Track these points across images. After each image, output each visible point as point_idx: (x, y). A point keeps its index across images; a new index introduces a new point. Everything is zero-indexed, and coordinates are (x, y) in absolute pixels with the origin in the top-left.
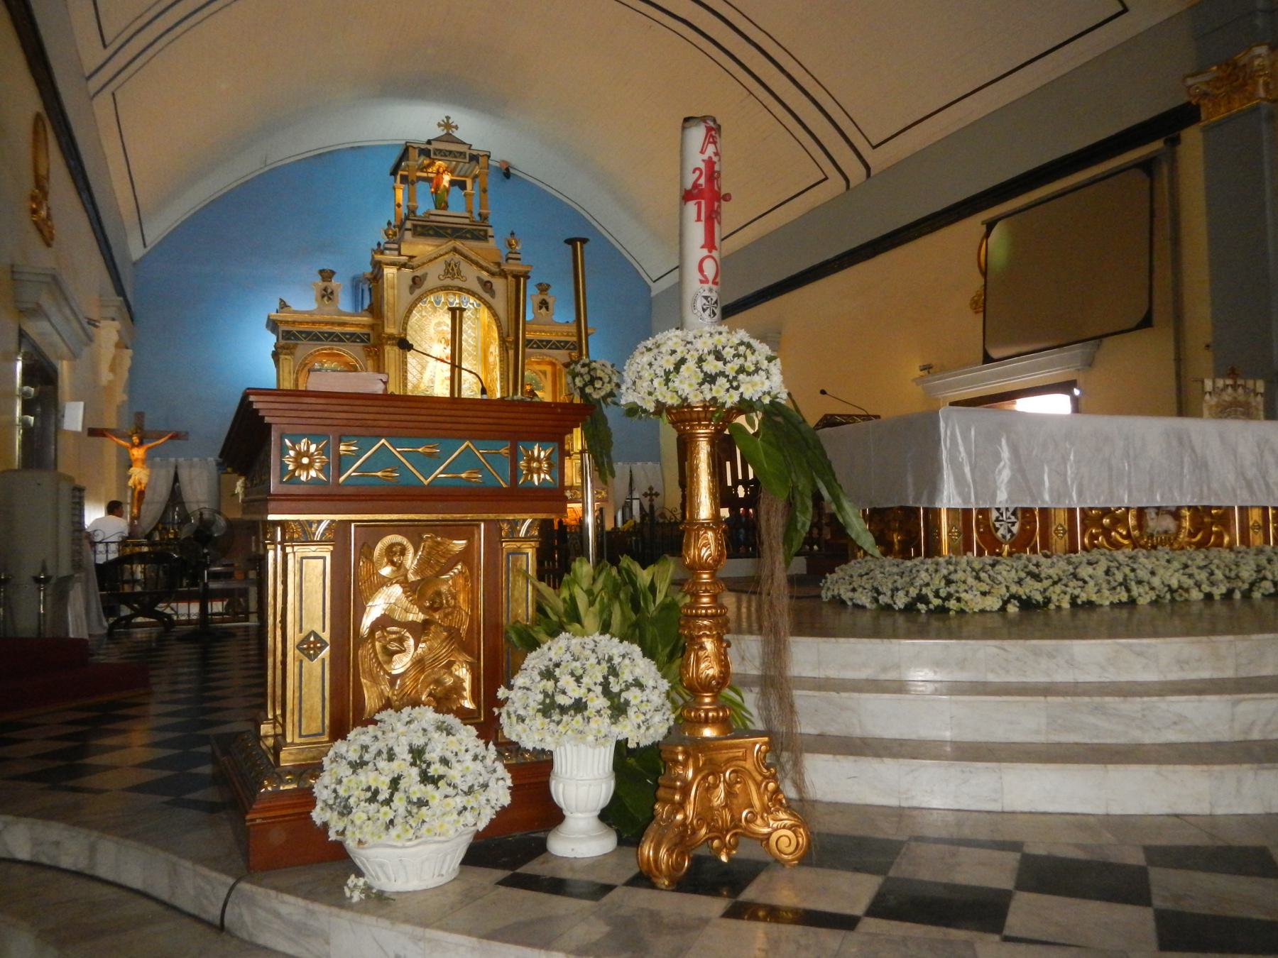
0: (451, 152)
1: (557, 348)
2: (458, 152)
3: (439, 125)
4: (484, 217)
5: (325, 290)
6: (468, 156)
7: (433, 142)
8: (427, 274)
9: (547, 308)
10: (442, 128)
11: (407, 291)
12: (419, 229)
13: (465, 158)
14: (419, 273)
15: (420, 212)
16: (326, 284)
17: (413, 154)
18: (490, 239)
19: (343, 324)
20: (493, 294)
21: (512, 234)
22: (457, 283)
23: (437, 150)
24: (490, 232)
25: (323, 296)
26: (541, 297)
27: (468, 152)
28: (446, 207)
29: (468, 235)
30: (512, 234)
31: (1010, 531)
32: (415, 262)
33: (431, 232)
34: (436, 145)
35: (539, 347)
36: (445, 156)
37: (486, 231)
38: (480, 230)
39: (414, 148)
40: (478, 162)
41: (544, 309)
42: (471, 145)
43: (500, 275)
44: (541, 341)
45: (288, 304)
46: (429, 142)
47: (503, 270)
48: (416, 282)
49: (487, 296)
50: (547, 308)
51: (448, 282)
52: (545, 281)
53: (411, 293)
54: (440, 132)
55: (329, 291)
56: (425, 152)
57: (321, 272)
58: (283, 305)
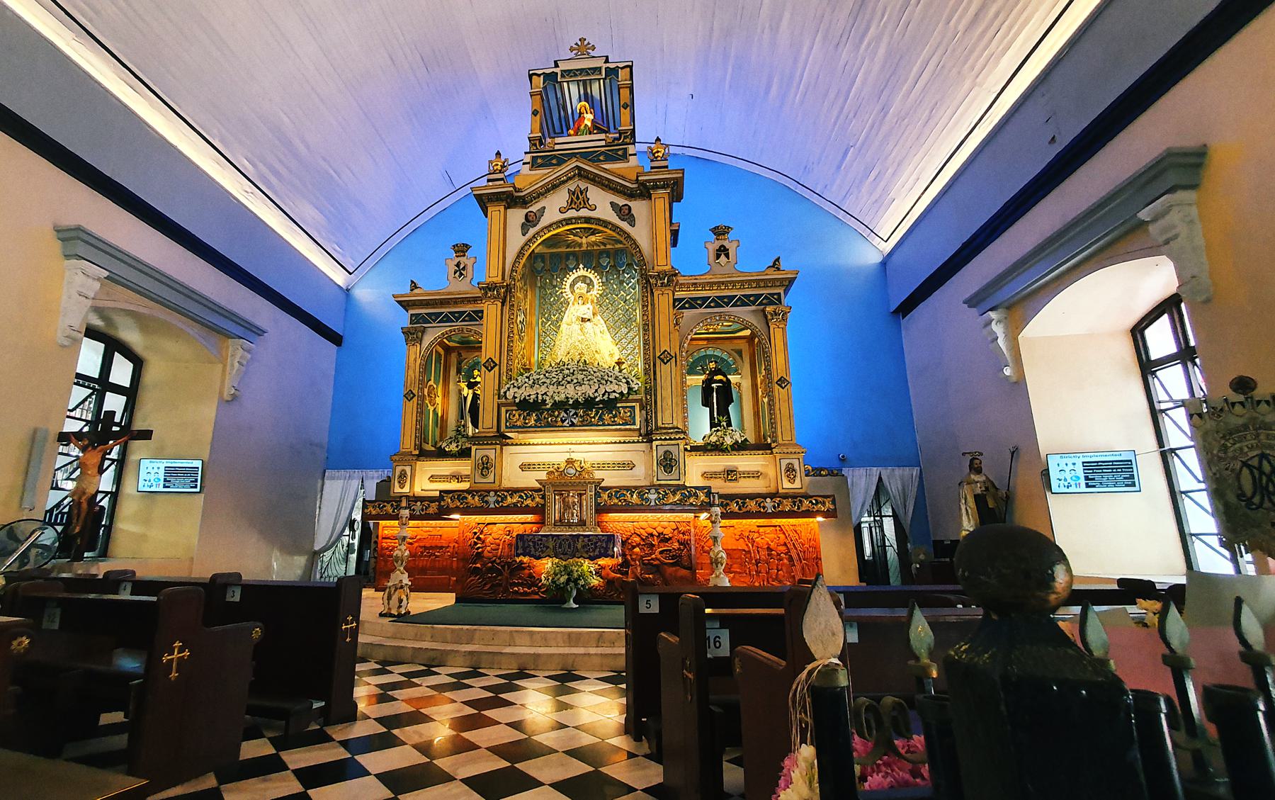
1: (744, 304)
2: (590, 69)
5: (458, 265)
8: (544, 208)
9: (727, 256)
10: (574, 52)
12: (539, 161)
13: (600, 73)
16: (459, 259)
20: (632, 224)
22: (584, 213)
23: (565, 71)
26: (718, 244)
29: (601, 158)
33: (554, 161)
35: (718, 306)
39: (539, 75)
41: (723, 258)
42: (607, 57)
44: (721, 298)
49: (624, 225)
50: (727, 256)
57: (454, 246)
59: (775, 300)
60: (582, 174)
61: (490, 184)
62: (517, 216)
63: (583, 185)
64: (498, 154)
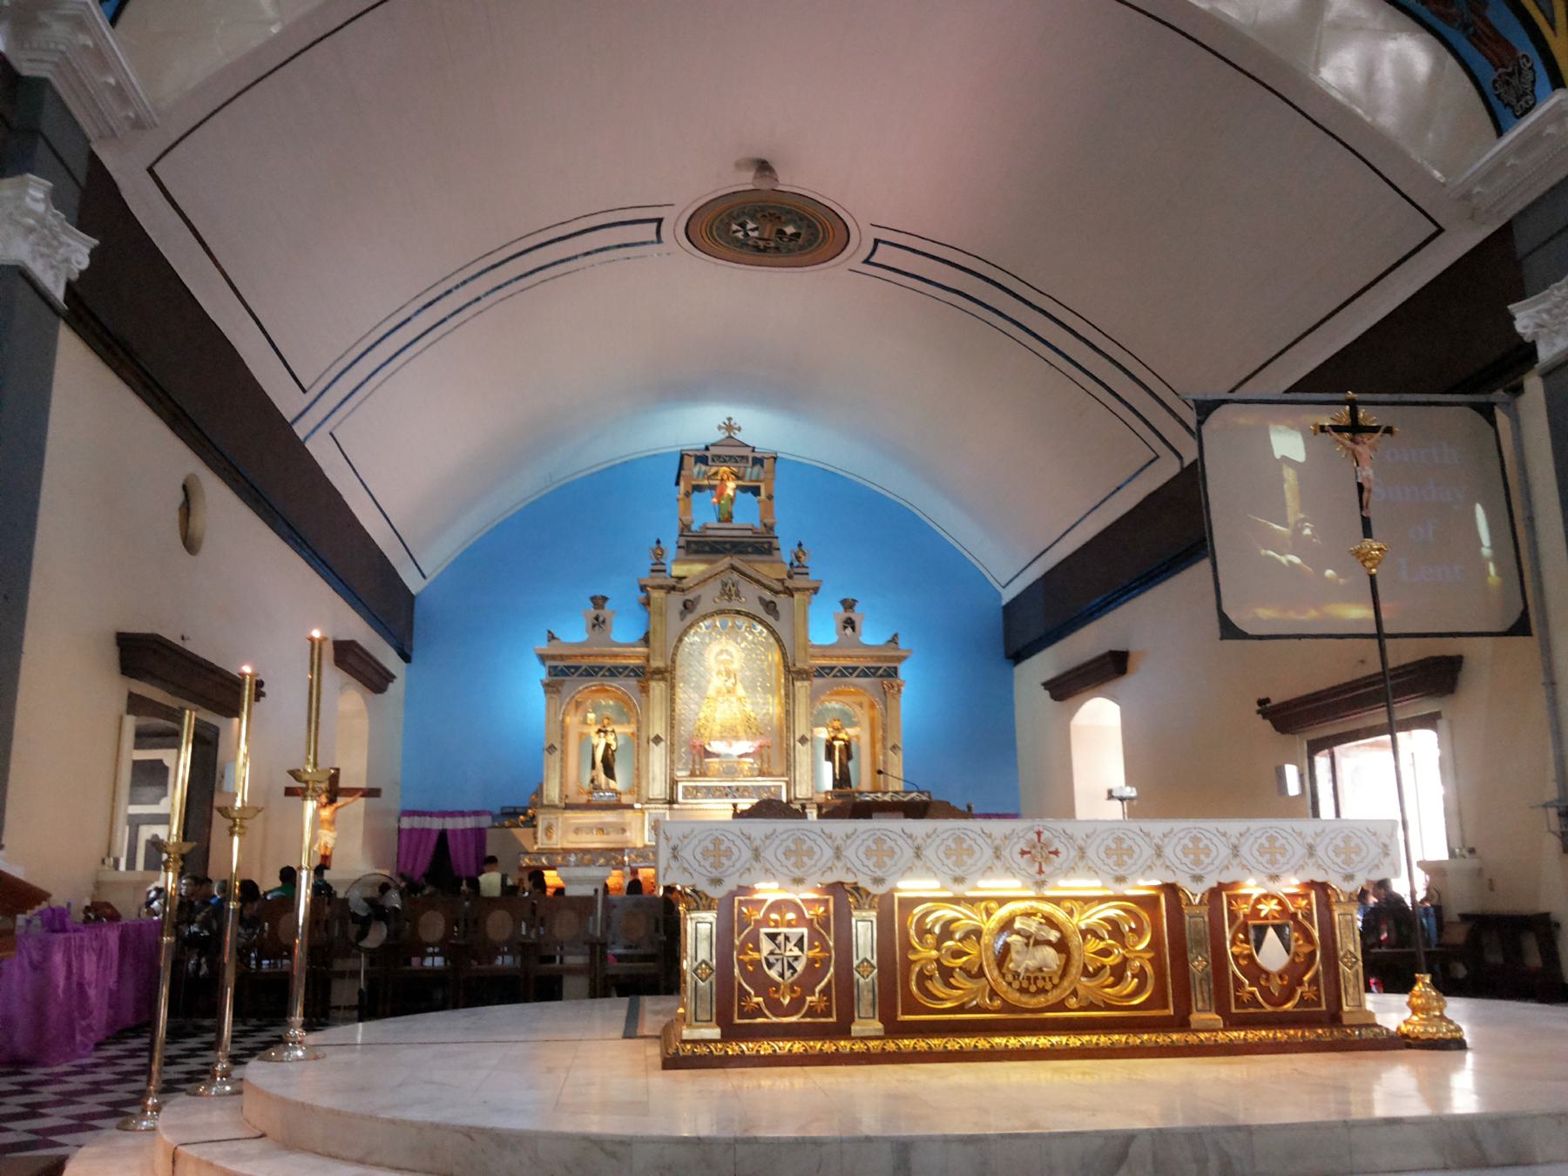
0: (731, 457)
1: (866, 675)
3: (720, 428)
4: (769, 528)
5: (597, 618)
6: (750, 460)
7: (711, 448)
8: (700, 596)
9: (853, 629)
11: (678, 616)
12: (693, 546)
13: (748, 461)
14: (690, 596)
15: (695, 527)
16: (599, 612)
17: (689, 461)
18: (775, 552)
19: (616, 656)
21: (800, 545)
23: (715, 456)
24: (776, 543)
25: (594, 626)
27: (751, 455)
28: (729, 518)
29: (750, 550)
30: (800, 545)
31: (791, 966)
32: (685, 584)
33: (707, 548)
34: (714, 451)
35: (844, 675)
36: (725, 461)
37: (770, 543)
38: (763, 543)
40: (762, 466)
41: (849, 631)
43: (785, 593)
44: (846, 668)
45: (556, 635)
46: (707, 448)
47: (787, 588)
48: (688, 607)
49: (770, 619)
50: (853, 629)
51: (725, 605)
52: (850, 596)
53: (682, 620)
54: (720, 436)
55: (601, 619)
56: (702, 460)
57: (593, 599)
58: (552, 637)
59: (892, 673)
60: (733, 568)
61: (654, 574)
62: (676, 600)
63: (735, 576)
64: (658, 542)
